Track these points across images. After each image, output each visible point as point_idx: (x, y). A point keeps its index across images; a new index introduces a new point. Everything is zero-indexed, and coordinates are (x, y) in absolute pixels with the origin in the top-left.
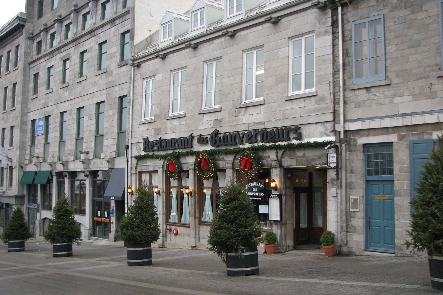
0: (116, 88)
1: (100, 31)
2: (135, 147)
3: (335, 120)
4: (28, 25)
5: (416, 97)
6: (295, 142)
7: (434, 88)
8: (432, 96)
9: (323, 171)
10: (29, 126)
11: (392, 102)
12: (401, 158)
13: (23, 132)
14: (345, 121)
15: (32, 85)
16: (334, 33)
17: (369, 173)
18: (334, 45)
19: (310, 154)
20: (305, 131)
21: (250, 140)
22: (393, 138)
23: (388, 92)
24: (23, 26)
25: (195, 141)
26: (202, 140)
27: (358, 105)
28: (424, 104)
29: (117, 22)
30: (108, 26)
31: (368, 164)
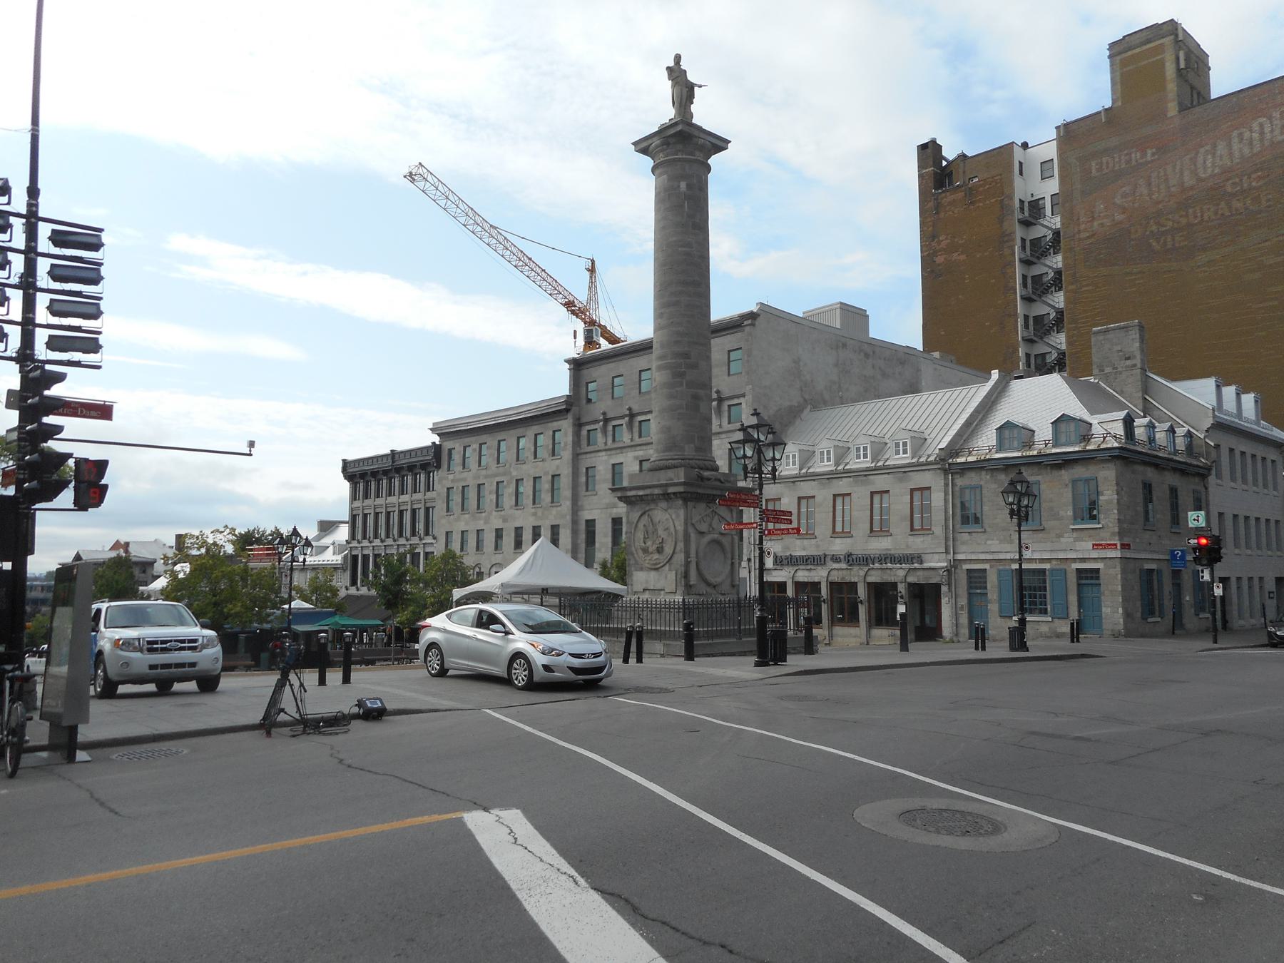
3: (947, 552)
6: (916, 565)
9: (937, 587)
10: (583, 527)
12: (992, 580)
13: (575, 532)
15: (583, 479)
16: (946, 494)
19: (926, 573)
20: (925, 557)
21: (880, 562)
22: (987, 566)
23: (984, 537)
24: (567, 410)
25: (828, 559)
26: (836, 559)
27: (963, 543)
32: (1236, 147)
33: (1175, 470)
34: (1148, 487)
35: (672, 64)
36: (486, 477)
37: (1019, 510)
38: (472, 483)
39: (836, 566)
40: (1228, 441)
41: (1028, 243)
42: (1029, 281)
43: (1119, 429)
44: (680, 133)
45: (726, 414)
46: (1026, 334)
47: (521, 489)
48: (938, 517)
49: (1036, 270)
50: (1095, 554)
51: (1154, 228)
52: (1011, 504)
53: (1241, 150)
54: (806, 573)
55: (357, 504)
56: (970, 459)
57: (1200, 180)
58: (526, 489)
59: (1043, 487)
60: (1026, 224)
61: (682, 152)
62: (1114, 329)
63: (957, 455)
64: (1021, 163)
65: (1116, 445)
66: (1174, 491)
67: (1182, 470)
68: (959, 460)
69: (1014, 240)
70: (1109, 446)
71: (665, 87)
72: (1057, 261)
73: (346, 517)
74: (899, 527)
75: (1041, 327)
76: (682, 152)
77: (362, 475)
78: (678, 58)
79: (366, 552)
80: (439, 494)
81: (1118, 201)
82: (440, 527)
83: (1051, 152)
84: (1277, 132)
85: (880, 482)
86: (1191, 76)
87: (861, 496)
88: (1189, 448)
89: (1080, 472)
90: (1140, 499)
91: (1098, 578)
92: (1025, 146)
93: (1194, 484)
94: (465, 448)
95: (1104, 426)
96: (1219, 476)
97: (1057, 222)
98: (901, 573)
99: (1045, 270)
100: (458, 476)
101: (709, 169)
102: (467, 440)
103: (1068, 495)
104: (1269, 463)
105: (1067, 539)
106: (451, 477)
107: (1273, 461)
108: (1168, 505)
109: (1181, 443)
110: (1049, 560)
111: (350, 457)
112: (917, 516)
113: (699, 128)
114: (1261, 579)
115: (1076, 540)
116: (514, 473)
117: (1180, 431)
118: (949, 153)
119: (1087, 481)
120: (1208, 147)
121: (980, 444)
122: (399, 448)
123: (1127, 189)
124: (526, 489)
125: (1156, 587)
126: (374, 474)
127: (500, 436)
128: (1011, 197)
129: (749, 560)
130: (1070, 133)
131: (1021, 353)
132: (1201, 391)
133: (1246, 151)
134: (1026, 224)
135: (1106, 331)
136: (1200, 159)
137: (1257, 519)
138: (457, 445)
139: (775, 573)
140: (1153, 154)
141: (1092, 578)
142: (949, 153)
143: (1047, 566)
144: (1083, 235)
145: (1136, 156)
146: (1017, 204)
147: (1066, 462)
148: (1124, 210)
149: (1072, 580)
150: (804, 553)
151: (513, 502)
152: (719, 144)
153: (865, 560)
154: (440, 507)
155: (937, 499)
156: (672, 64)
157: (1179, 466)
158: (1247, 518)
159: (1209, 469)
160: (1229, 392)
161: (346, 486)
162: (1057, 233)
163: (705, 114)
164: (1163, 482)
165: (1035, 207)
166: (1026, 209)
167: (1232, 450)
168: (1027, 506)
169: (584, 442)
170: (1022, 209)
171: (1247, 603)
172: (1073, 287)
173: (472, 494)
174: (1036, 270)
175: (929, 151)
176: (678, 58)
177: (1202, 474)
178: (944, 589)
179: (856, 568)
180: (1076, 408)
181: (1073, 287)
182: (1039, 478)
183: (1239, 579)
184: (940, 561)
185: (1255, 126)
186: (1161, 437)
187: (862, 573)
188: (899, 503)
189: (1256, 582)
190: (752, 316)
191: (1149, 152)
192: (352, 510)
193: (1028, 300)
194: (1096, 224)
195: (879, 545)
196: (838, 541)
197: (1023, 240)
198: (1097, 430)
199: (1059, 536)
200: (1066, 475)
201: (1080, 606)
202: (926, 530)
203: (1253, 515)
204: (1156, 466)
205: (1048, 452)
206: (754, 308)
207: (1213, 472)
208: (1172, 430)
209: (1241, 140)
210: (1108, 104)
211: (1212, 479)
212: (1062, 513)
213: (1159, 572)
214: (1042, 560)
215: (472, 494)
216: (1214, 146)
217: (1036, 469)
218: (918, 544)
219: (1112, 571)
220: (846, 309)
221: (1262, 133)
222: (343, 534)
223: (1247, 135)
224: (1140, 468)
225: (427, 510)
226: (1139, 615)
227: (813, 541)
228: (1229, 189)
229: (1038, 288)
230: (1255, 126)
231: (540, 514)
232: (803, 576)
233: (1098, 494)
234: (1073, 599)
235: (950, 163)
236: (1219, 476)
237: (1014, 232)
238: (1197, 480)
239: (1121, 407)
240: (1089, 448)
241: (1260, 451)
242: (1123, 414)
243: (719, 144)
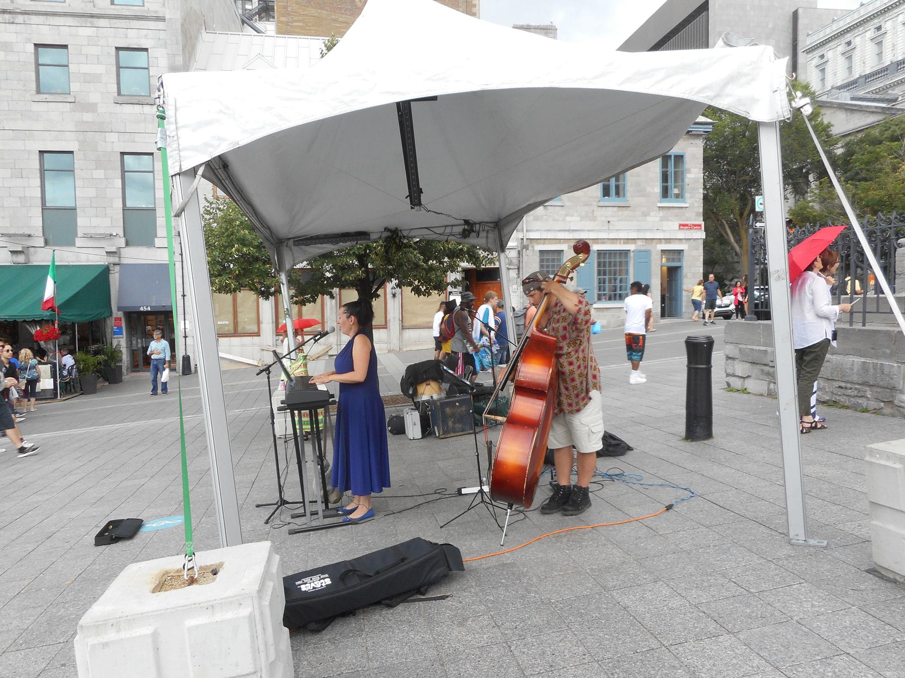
0: (113, 137)
1: (35, 19)
5: (582, 218)
7: (596, 214)
8: (594, 219)
11: (564, 220)
14: (527, 231)
23: (562, 212)
28: (589, 225)
30: (70, 21)
50: (681, 235)
115: (662, 219)
143: (631, 247)
199: (646, 214)
212: (649, 189)
214: (627, 241)
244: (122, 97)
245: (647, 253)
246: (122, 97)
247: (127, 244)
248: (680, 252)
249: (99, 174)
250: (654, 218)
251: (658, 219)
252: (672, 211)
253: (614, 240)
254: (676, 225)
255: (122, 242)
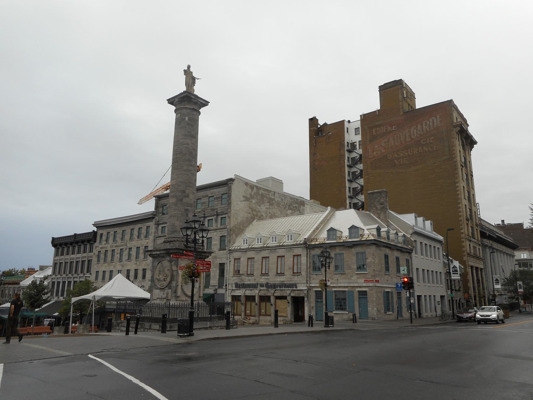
0: (218, 259)
2: (230, 286)
3: (307, 283)
4: (157, 218)
6: (294, 288)
9: (303, 298)
16: (307, 257)
17: (316, 299)
18: (307, 260)
19: (299, 292)
20: (298, 285)
21: (280, 287)
24: (153, 218)
25: (259, 285)
26: (262, 285)
27: (314, 279)
29: (218, 231)
31: (316, 296)
32: (424, 127)
33: (398, 250)
34: (386, 257)
35: (186, 69)
36: (116, 246)
37: (325, 264)
38: (110, 249)
39: (262, 288)
40: (419, 239)
41: (350, 159)
42: (351, 174)
43: (375, 232)
44: (186, 96)
45: (220, 221)
46: (349, 195)
47: (131, 252)
48: (304, 267)
49: (354, 170)
50: (365, 285)
51: (396, 156)
52: (322, 261)
53: (426, 129)
54: (250, 292)
55: (57, 258)
56: (317, 243)
57: (412, 139)
58: (134, 252)
59: (345, 255)
60: (350, 151)
61: (188, 105)
62: (376, 192)
63: (312, 242)
64: (347, 128)
65: (373, 238)
66: (398, 259)
67: (401, 250)
68: (313, 243)
69: (345, 157)
70: (370, 239)
71: (183, 78)
72: (361, 166)
73: (52, 265)
74: (288, 273)
75: (356, 192)
76: (188, 105)
77: (60, 244)
78: (189, 67)
79: (59, 280)
80: (94, 254)
81: (383, 145)
82: (94, 269)
83: (358, 125)
84: (439, 123)
85: (281, 252)
86: (408, 100)
87: (273, 258)
88: (404, 242)
89: (359, 249)
90: (383, 262)
91: (366, 295)
92: (349, 122)
93: (406, 256)
94: (108, 233)
95: (369, 230)
96: (416, 253)
97: (360, 151)
98: (289, 292)
99: (356, 170)
100: (103, 246)
101: (200, 113)
102: (109, 230)
103: (354, 259)
104: (437, 249)
105: (355, 278)
106: (100, 246)
107: (438, 248)
108: (395, 264)
109: (401, 239)
110: (347, 287)
111: (55, 237)
112: (295, 267)
113: (196, 96)
114: (434, 296)
115: (358, 278)
116: (128, 245)
117: (400, 234)
118: (321, 123)
119: (362, 253)
120: (415, 127)
121: (321, 237)
122: (78, 232)
123: (386, 140)
124: (134, 252)
125: (390, 299)
126: (66, 244)
127: (124, 228)
128: (344, 140)
129: (226, 285)
130: (365, 118)
131: (348, 202)
132: (409, 219)
133: (428, 129)
134: (350, 151)
135: (373, 193)
136: (412, 131)
137: (432, 271)
138: (104, 232)
139: (237, 291)
140: (395, 128)
141: (364, 295)
142: (321, 123)
143: (346, 289)
144: (371, 157)
145: (389, 128)
146: (346, 144)
147: (354, 245)
148: (385, 149)
149: (356, 296)
150: (249, 283)
151: (127, 258)
152: (205, 103)
153: (274, 286)
154: (95, 259)
155: (304, 259)
156: (186, 69)
157: (399, 248)
158: (428, 271)
159: (412, 250)
160: (420, 220)
161: (53, 249)
162: (361, 156)
163: (199, 91)
164: (393, 255)
165: (353, 145)
166: (350, 146)
167: (421, 243)
168: (329, 263)
169: (160, 232)
170: (348, 146)
171: (429, 306)
172: (366, 177)
173: (109, 254)
174: (354, 170)
175: (313, 121)
176: (189, 67)
177: (409, 252)
178: (306, 299)
179: (270, 290)
180: (358, 223)
181: (366, 177)
182: (343, 252)
183: (425, 296)
184: (304, 287)
185: (431, 120)
186: (392, 236)
187: (273, 292)
188: (289, 261)
189: (432, 297)
190: (231, 180)
191: (394, 127)
192: (54, 260)
193: (350, 181)
194: (375, 153)
195: (279, 280)
196: (263, 277)
197: (348, 158)
198: (366, 232)
199: (352, 276)
200: (354, 250)
201: (360, 306)
202: (299, 273)
203: (430, 270)
204: (390, 248)
205: (347, 240)
206: (233, 177)
207: (414, 251)
208: (397, 234)
209: (426, 125)
210: (379, 108)
211: (413, 254)
213: (392, 292)
214: (345, 287)
215: (109, 254)
216: (417, 127)
217: (342, 248)
218: (296, 279)
219: (371, 292)
220: (273, 179)
221: (433, 123)
222: (49, 272)
223: (428, 123)
224: (383, 249)
225: (89, 261)
226: (383, 311)
227: (253, 277)
228: (422, 142)
229: (354, 177)
230: (431, 120)
231: (138, 263)
232: (248, 293)
233: (366, 259)
234: (356, 304)
235: (321, 126)
236: (416, 253)
237: (345, 155)
238: (407, 254)
239: (376, 222)
240: (363, 239)
241: (433, 244)
242: (376, 226)
243: (205, 103)
244: (221, 249)
245: (353, 292)
246: (221, 249)
247: (219, 288)
248: (366, 291)
249: (215, 269)
250: (355, 278)
251: (356, 278)
252: (361, 275)
253: (340, 287)
254: (363, 281)
255: (217, 287)
